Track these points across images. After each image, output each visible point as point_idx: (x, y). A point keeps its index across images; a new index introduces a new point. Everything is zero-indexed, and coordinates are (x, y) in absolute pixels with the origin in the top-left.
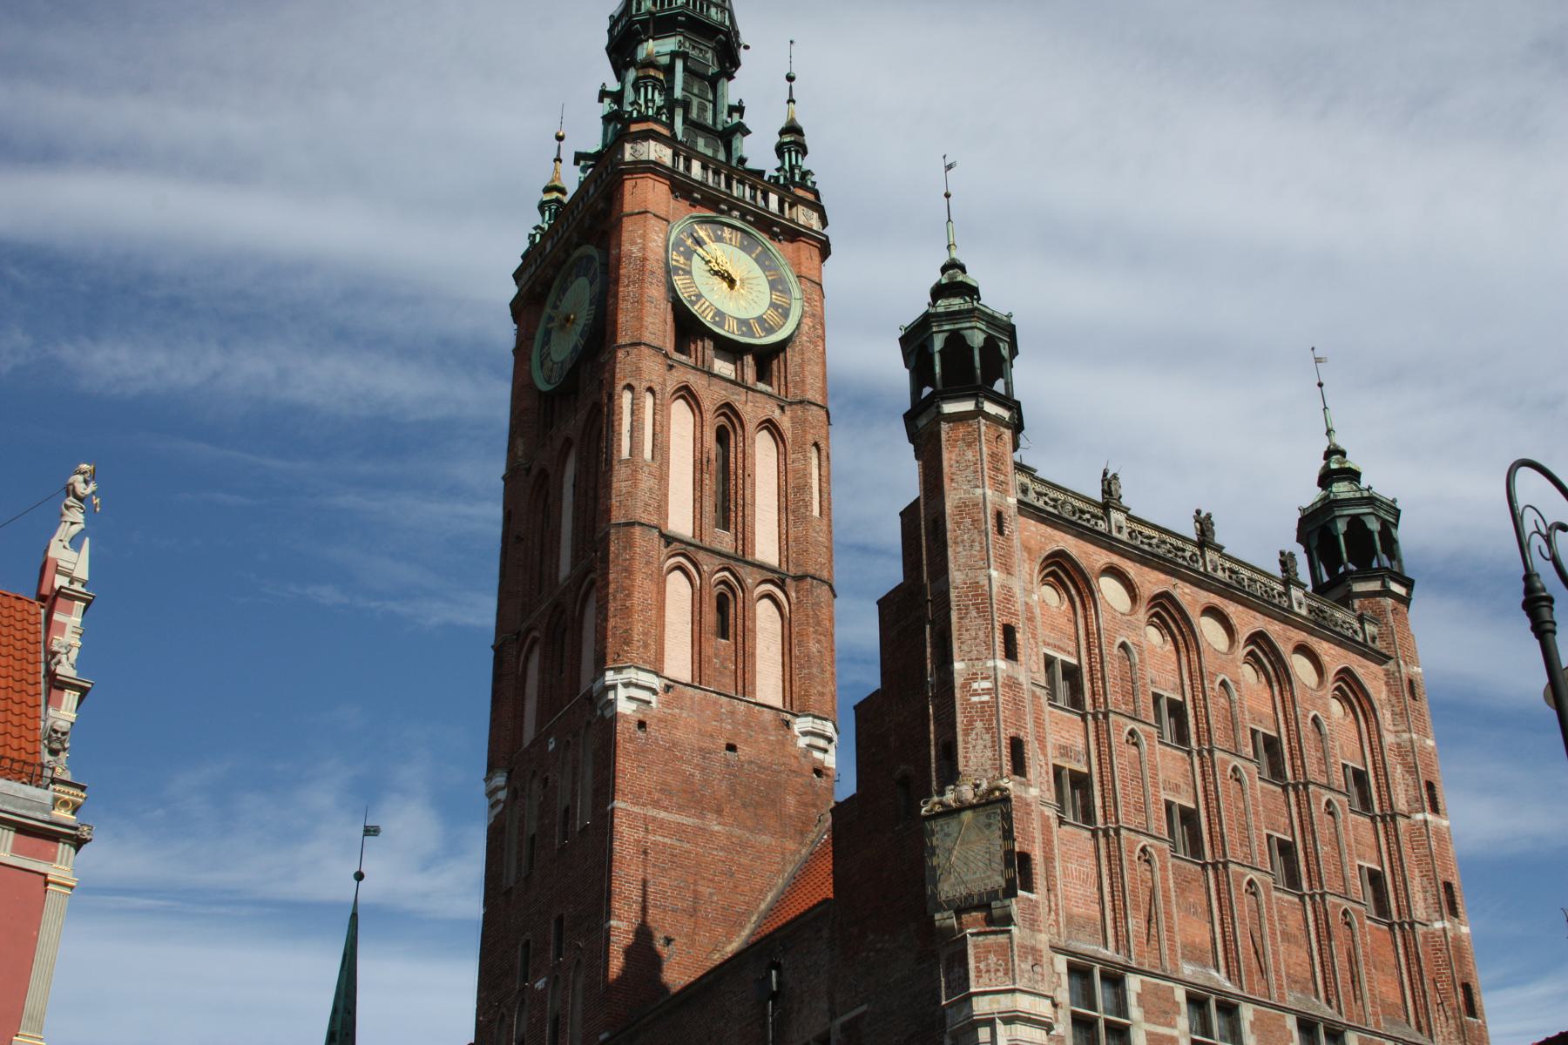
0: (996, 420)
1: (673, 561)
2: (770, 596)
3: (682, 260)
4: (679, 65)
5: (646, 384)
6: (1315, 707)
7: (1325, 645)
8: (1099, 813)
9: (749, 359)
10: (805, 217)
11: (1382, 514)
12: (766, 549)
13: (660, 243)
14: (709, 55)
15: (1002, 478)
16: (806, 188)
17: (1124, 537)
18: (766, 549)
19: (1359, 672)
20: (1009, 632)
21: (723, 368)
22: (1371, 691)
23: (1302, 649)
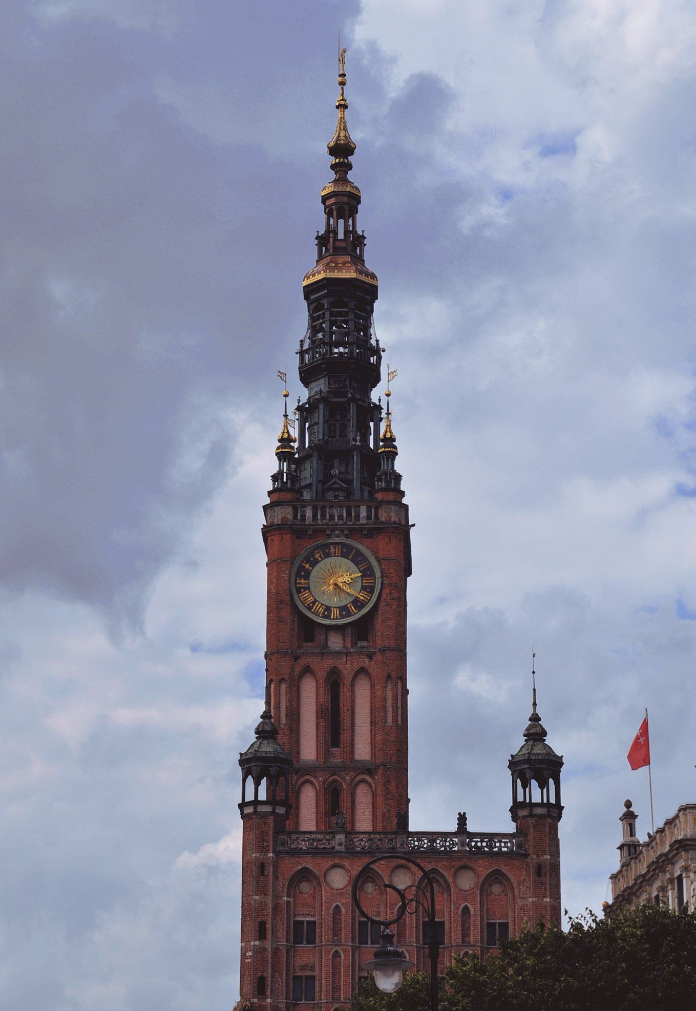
0: (264, 815)
1: (302, 780)
2: (363, 781)
3: (303, 581)
4: (321, 407)
5: (280, 678)
6: (466, 901)
7: (481, 862)
8: (317, 995)
9: (349, 631)
10: (383, 517)
11: (537, 766)
12: (363, 751)
13: (285, 576)
14: (347, 382)
15: (266, 844)
16: (387, 489)
17: (342, 848)
18: (363, 751)
19: (504, 869)
20: (262, 925)
21: (335, 642)
22: (512, 878)
23: (465, 867)
